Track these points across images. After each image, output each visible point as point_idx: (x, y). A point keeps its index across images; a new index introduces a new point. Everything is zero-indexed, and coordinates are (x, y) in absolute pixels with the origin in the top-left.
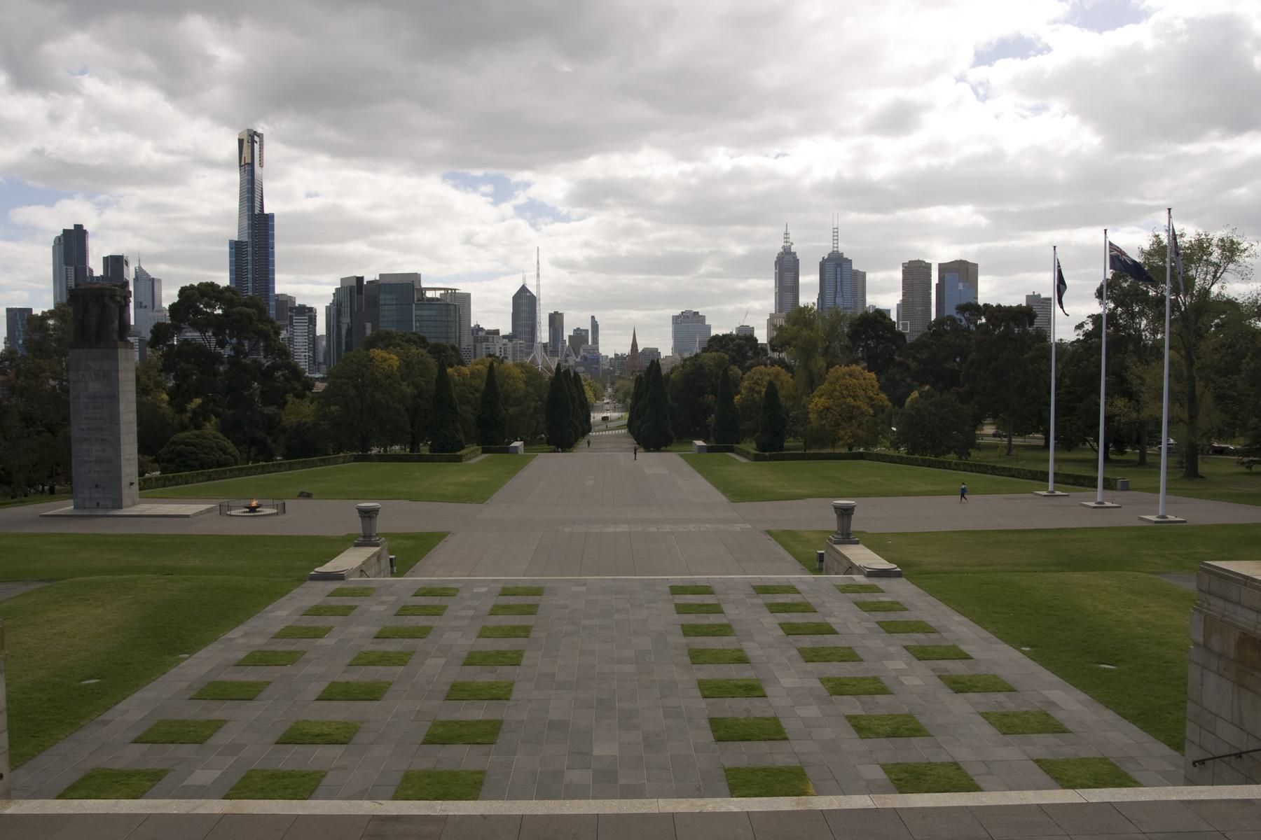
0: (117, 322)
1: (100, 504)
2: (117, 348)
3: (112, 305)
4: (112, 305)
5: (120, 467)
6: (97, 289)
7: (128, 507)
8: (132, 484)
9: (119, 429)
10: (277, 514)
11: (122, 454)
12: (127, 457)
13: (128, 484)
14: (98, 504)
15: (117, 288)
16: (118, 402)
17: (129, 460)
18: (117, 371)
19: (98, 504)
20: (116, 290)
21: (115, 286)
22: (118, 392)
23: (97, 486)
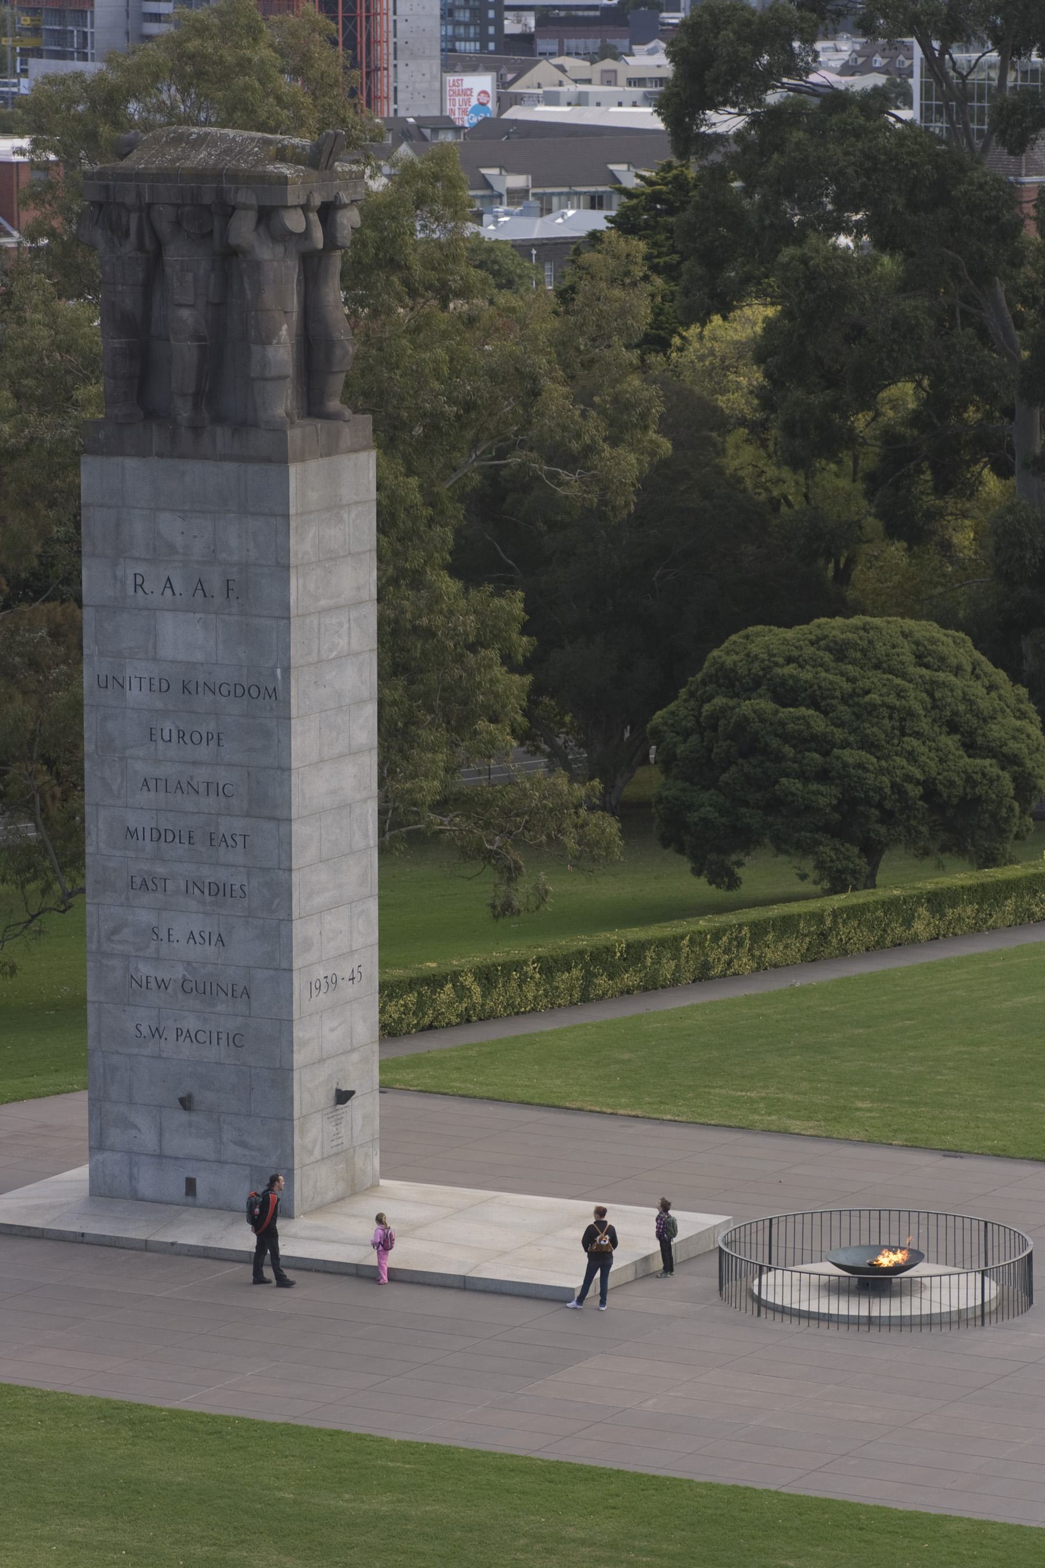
0: (286, 333)
1: (199, 1184)
2: (283, 460)
3: (266, 252)
4: (266, 252)
5: (284, 1024)
6: (199, 175)
7: (321, 1208)
8: (343, 1097)
9: (285, 843)
10: (982, 1315)
11: (297, 963)
12: (320, 972)
13: (325, 1096)
14: (191, 1185)
15: (286, 170)
16: (286, 718)
17: (332, 983)
18: (283, 568)
19: (191, 1185)
20: (283, 181)
21: (281, 155)
22: (287, 670)
23: (186, 1103)
